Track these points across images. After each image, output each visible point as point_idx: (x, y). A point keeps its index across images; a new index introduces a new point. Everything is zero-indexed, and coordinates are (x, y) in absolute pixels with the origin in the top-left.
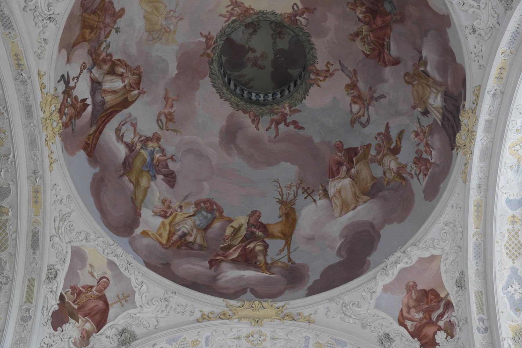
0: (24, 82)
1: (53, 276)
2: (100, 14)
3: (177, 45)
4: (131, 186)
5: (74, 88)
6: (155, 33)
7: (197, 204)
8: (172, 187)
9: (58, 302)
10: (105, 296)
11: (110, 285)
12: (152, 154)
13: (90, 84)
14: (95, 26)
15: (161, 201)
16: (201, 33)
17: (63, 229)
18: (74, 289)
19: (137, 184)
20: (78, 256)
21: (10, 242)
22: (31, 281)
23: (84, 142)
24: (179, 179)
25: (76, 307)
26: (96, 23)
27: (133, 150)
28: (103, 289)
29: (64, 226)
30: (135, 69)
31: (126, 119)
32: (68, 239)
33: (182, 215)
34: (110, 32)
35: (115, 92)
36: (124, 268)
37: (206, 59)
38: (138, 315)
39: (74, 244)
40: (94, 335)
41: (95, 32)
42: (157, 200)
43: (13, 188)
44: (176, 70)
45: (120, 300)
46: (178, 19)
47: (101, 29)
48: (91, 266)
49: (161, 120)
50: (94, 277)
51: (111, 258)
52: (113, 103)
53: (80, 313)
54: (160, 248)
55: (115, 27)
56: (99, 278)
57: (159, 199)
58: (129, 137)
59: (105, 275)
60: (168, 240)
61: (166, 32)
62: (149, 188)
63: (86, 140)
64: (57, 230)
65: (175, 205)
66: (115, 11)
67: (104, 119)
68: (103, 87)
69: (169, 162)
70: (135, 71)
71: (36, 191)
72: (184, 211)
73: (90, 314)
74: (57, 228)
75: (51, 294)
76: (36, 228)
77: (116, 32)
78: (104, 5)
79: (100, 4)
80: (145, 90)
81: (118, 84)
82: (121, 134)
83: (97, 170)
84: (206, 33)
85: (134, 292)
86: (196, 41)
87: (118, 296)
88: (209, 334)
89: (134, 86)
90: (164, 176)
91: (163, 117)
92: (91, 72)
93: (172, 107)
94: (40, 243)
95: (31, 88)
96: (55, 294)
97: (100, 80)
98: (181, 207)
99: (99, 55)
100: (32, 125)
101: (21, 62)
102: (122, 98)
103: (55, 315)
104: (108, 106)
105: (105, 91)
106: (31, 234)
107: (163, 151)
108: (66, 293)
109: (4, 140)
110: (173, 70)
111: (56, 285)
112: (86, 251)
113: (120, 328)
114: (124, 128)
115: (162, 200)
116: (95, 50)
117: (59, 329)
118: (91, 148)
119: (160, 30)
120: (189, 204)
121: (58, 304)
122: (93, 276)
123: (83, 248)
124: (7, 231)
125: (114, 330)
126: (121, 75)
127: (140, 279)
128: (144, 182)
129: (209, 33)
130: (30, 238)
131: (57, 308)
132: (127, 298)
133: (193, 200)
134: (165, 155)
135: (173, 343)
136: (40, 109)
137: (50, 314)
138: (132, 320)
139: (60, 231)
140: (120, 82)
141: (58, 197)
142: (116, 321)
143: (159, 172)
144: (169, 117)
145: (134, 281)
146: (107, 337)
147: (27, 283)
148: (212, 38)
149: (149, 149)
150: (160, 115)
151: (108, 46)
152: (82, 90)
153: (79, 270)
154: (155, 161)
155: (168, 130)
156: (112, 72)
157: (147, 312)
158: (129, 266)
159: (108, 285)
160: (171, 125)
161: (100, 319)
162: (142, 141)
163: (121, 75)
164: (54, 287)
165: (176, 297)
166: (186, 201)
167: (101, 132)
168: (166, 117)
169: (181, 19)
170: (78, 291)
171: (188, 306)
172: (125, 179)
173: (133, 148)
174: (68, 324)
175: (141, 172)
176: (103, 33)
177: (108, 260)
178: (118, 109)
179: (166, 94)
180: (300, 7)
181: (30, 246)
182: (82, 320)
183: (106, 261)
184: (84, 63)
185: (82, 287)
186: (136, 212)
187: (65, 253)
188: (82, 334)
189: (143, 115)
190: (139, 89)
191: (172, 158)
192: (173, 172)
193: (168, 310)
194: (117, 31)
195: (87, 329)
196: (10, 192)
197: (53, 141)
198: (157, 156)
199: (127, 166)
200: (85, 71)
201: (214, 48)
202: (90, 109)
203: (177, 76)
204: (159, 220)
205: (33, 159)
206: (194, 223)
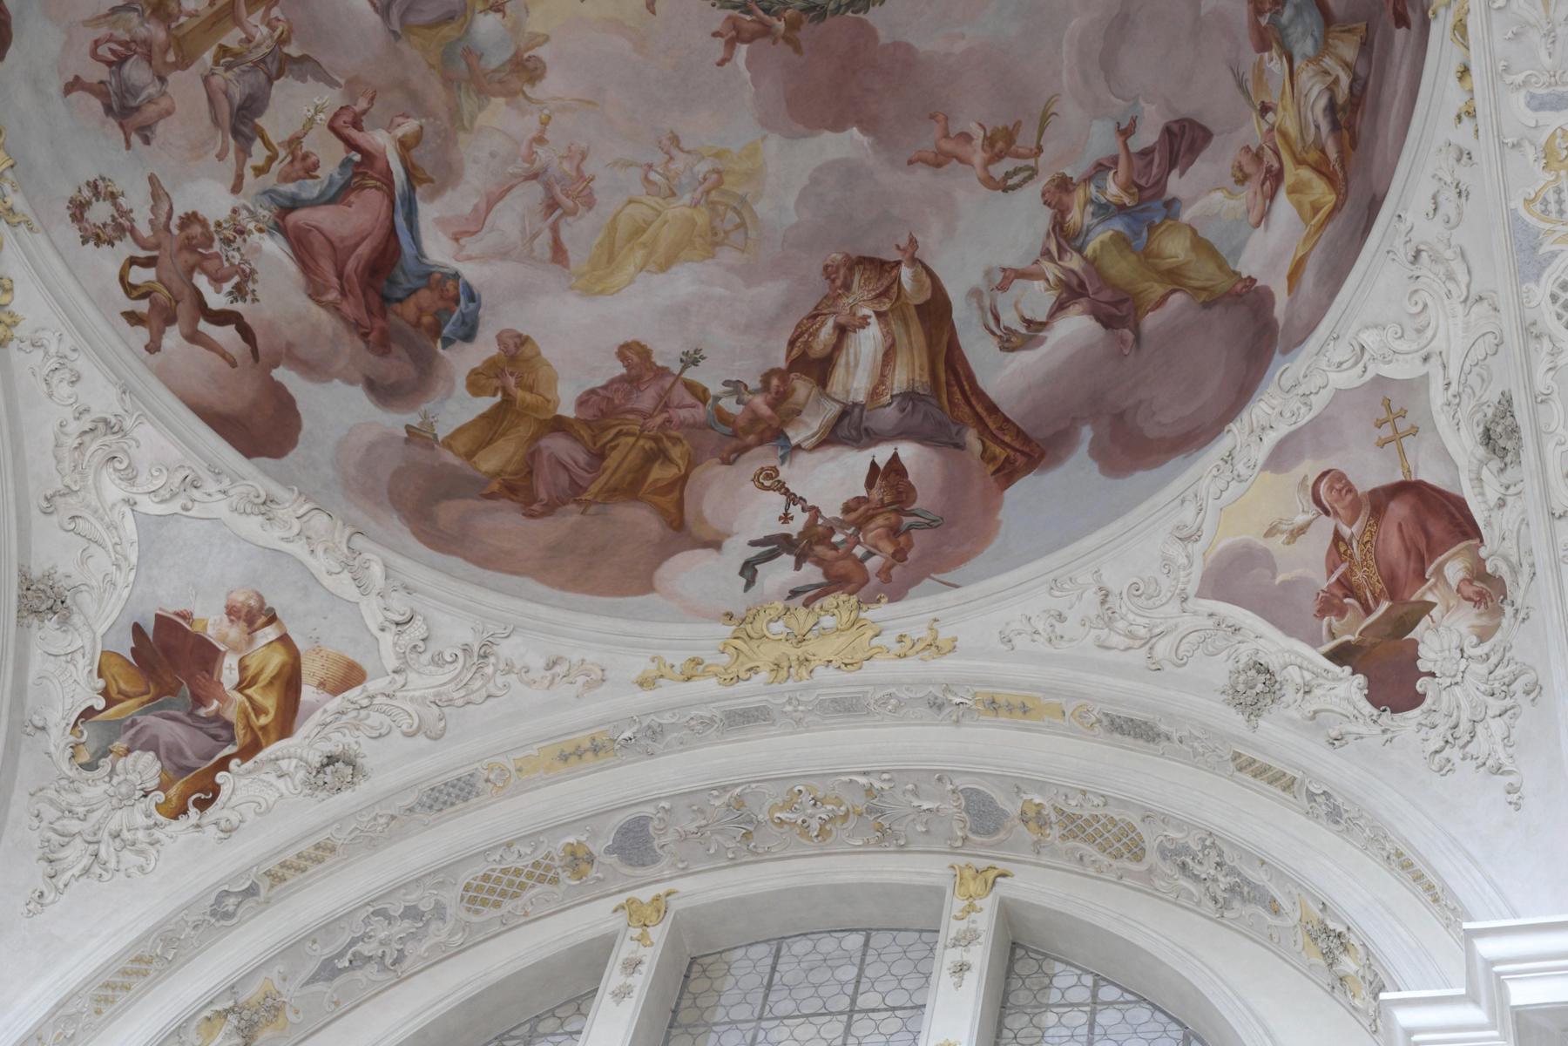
0: (656, 733)
1: (1262, 678)
2: (614, 431)
3: (764, 138)
4: (1177, 299)
5: (815, 511)
6: (722, 220)
7: (1263, 45)
8: (1206, 135)
9: (1348, 669)
10: (1374, 492)
11: (1342, 469)
12: (1105, 210)
13: (832, 451)
14: (649, 445)
15: (1239, 188)
16: (721, 63)
17: (1140, 620)
18: (1329, 606)
19: (1174, 277)
20: (1235, 576)
21: (1113, 812)
22: (1244, 765)
23: (992, 479)
24: (1186, 109)
25: (1385, 605)
26: (641, 442)
27: (1082, 284)
28: (1349, 497)
29: (1131, 617)
30: (833, 281)
31: (981, 308)
32: (1173, 608)
33: (1284, 109)
34: (691, 387)
35: (889, 355)
36: (1304, 409)
37: (807, 32)
38: (1453, 373)
39: (1192, 588)
40: (1483, 552)
41: (668, 444)
42: (1232, 203)
43: (963, 783)
44: (846, 134)
45: (1397, 437)
46: (674, 152)
47: (669, 420)
48: (1271, 532)
49: (1008, 175)
50: (1309, 524)
51: (1261, 453)
52: (921, 359)
53: (1406, 595)
54: (1340, 218)
55: (676, 368)
56: (1314, 508)
57: (1231, 194)
58: (1037, 298)
59: (1310, 483)
60: (1330, 178)
61: (720, 182)
62: (1194, 232)
63: (991, 468)
64: (1138, 643)
65: (1253, 131)
66: (622, 379)
67: (959, 396)
68: (861, 398)
69: (1139, 142)
70: (838, 283)
71: (993, 705)
72: (1272, 98)
73: (1422, 556)
74: (1129, 642)
75: (1317, 692)
76: (1099, 721)
77: (695, 363)
78: (586, 423)
79: (577, 439)
80: (903, 241)
81: (868, 342)
82: (1023, 331)
83: (1087, 433)
84: (718, 47)
85: (1379, 380)
86: (748, 75)
87: (1382, 444)
88: (1520, 99)
89: (886, 283)
90: (1172, 165)
91: (998, 170)
92: (798, 447)
93: (966, 137)
94: (1138, 715)
95: (668, 715)
96: (1321, 681)
97: (833, 410)
98: (1265, 109)
99: (756, 418)
100: (789, 708)
101: (587, 744)
102: (916, 327)
103: (1374, 699)
104: (926, 378)
105: (874, 394)
106: (1117, 736)
107: (1101, 168)
108: (1333, 636)
109: (820, 795)
110: (849, 144)
111: (1293, 672)
112: (1220, 546)
113: (1481, 451)
114: (1010, 319)
115: (1237, 182)
116: (735, 435)
117: (1421, 684)
118: (1020, 450)
119: (712, 205)
120: (1260, 70)
121: (1353, 674)
122: (1302, 530)
123: (1212, 554)
124: (1086, 815)
125: (1485, 473)
126: (842, 331)
127: (1341, 352)
128: (1175, 248)
129: (715, 34)
130: (1128, 740)
131: (1360, 679)
132: (1392, 410)
133: (1249, 56)
134: (1115, 161)
135: (1546, 248)
136: (741, 686)
137: (1368, 708)
138: (1464, 397)
139: (1142, 632)
140: (862, 333)
141: (1040, 627)
142: (1461, 461)
143: (1161, 184)
144: (1000, 145)
145: (1345, 374)
146: (1502, 503)
147: (1246, 777)
148: (734, 23)
149: (1088, 220)
150: (989, 182)
151: (736, 387)
152: (833, 479)
153: (1274, 577)
154: (1127, 200)
155: (1040, 149)
156: (819, 368)
157: (1448, 340)
158: (1300, 390)
159: (1341, 477)
160: (1025, 140)
161: (1441, 517)
162: (1060, 248)
163: (842, 331)
164: (1299, 680)
165: (1409, 217)
166: (1250, 86)
167: (993, 409)
168: (998, 157)
169: (675, 140)
170: (1339, 593)
171: (1440, 174)
172: (1151, 321)
173: (1075, 282)
174: (1422, 650)
175: (1147, 256)
176: (684, 414)
177: (1266, 467)
178: (945, 338)
179: (926, 162)
181: (1151, 745)
182: (1430, 589)
183: (1268, 475)
184: (756, 479)
185: (1331, 572)
186: (1239, 295)
187: (1210, 623)
188: (1469, 599)
189: (983, 241)
190: (898, 263)
191: (1126, 133)
192: (1167, 130)
193: (1449, 254)
194: (692, 359)
195: (1461, 575)
196: (978, 792)
197: (870, 633)
198: (1113, 189)
199: (1118, 312)
200: (784, 472)
201: (767, 11)
202: (908, 452)
203: (869, 125)
204: (1284, 205)
205: (896, 709)
206: (1310, 60)
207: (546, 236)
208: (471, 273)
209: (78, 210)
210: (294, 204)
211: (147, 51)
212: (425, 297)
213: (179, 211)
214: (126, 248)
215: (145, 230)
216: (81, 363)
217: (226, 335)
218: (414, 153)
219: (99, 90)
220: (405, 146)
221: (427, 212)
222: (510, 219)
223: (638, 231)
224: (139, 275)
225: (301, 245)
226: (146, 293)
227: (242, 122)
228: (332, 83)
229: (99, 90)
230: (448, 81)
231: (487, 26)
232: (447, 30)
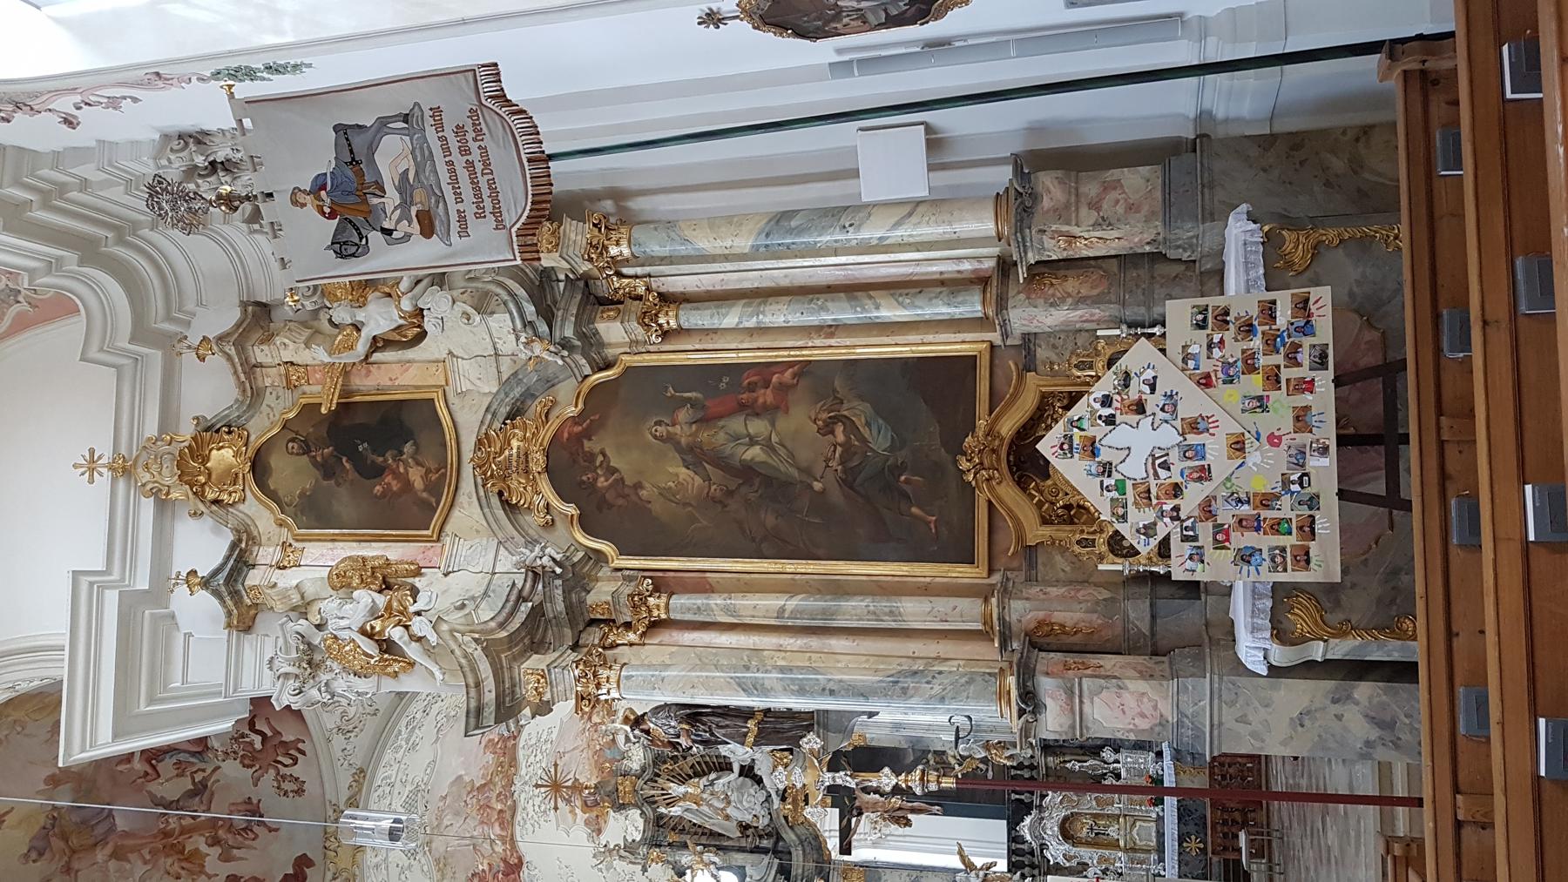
227: (200, 790)
228: (149, 793)
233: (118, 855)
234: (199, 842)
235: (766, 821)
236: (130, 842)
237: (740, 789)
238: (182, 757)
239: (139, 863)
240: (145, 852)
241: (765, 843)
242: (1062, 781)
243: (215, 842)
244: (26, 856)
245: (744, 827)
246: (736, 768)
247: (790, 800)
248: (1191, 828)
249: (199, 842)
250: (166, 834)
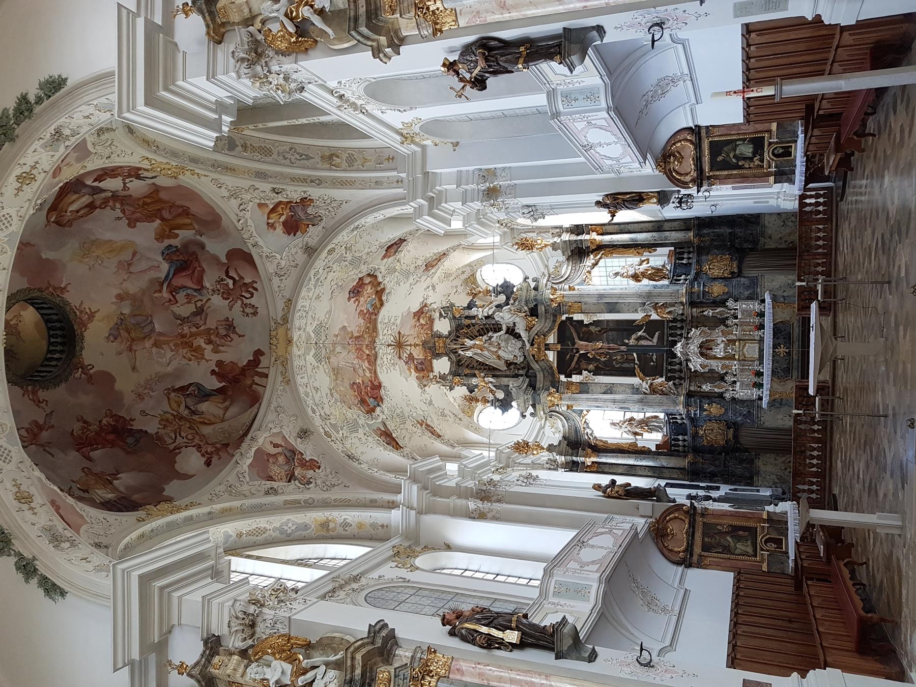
180: (91, 371)
207: (135, 258)
208: (160, 259)
209: (255, 314)
210: (195, 290)
211: (217, 335)
212: (175, 258)
213: (228, 302)
214: (246, 301)
215: (239, 302)
216: (277, 289)
217: (232, 273)
218: (159, 288)
219: (234, 332)
220: (160, 291)
221: (163, 276)
222: (143, 265)
223: (111, 251)
224: (248, 295)
225: (200, 281)
226: (248, 291)
229: (234, 332)
230: (142, 301)
231: (126, 311)
232: (137, 313)
233: (156, 344)
234: (200, 342)
235: (522, 359)
236: (162, 338)
237: (507, 341)
238: (189, 291)
239: (169, 350)
240: (171, 344)
241: (521, 372)
242: (697, 322)
243: (210, 342)
244: (108, 338)
245: (509, 364)
246: (504, 328)
247: (536, 346)
248: (781, 340)
249: (200, 342)
250: (183, 336)
